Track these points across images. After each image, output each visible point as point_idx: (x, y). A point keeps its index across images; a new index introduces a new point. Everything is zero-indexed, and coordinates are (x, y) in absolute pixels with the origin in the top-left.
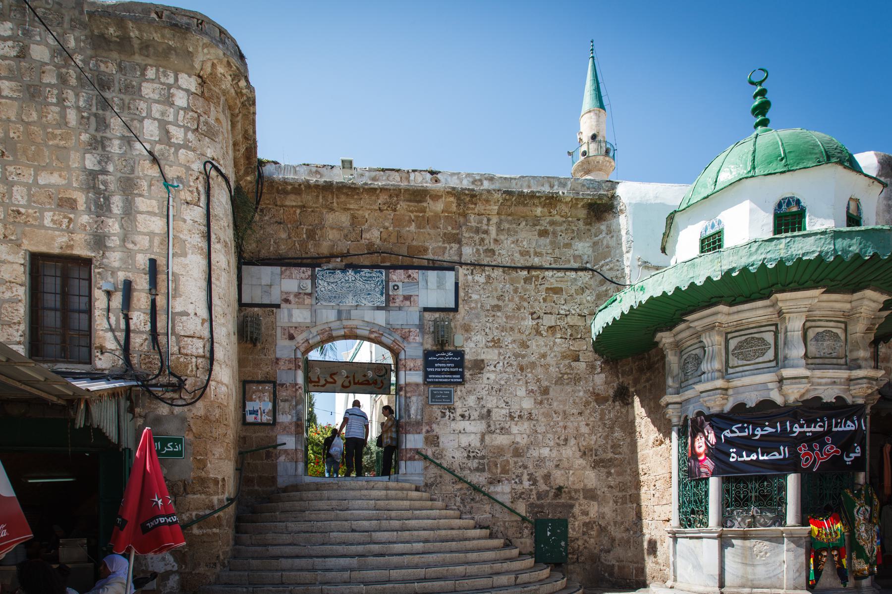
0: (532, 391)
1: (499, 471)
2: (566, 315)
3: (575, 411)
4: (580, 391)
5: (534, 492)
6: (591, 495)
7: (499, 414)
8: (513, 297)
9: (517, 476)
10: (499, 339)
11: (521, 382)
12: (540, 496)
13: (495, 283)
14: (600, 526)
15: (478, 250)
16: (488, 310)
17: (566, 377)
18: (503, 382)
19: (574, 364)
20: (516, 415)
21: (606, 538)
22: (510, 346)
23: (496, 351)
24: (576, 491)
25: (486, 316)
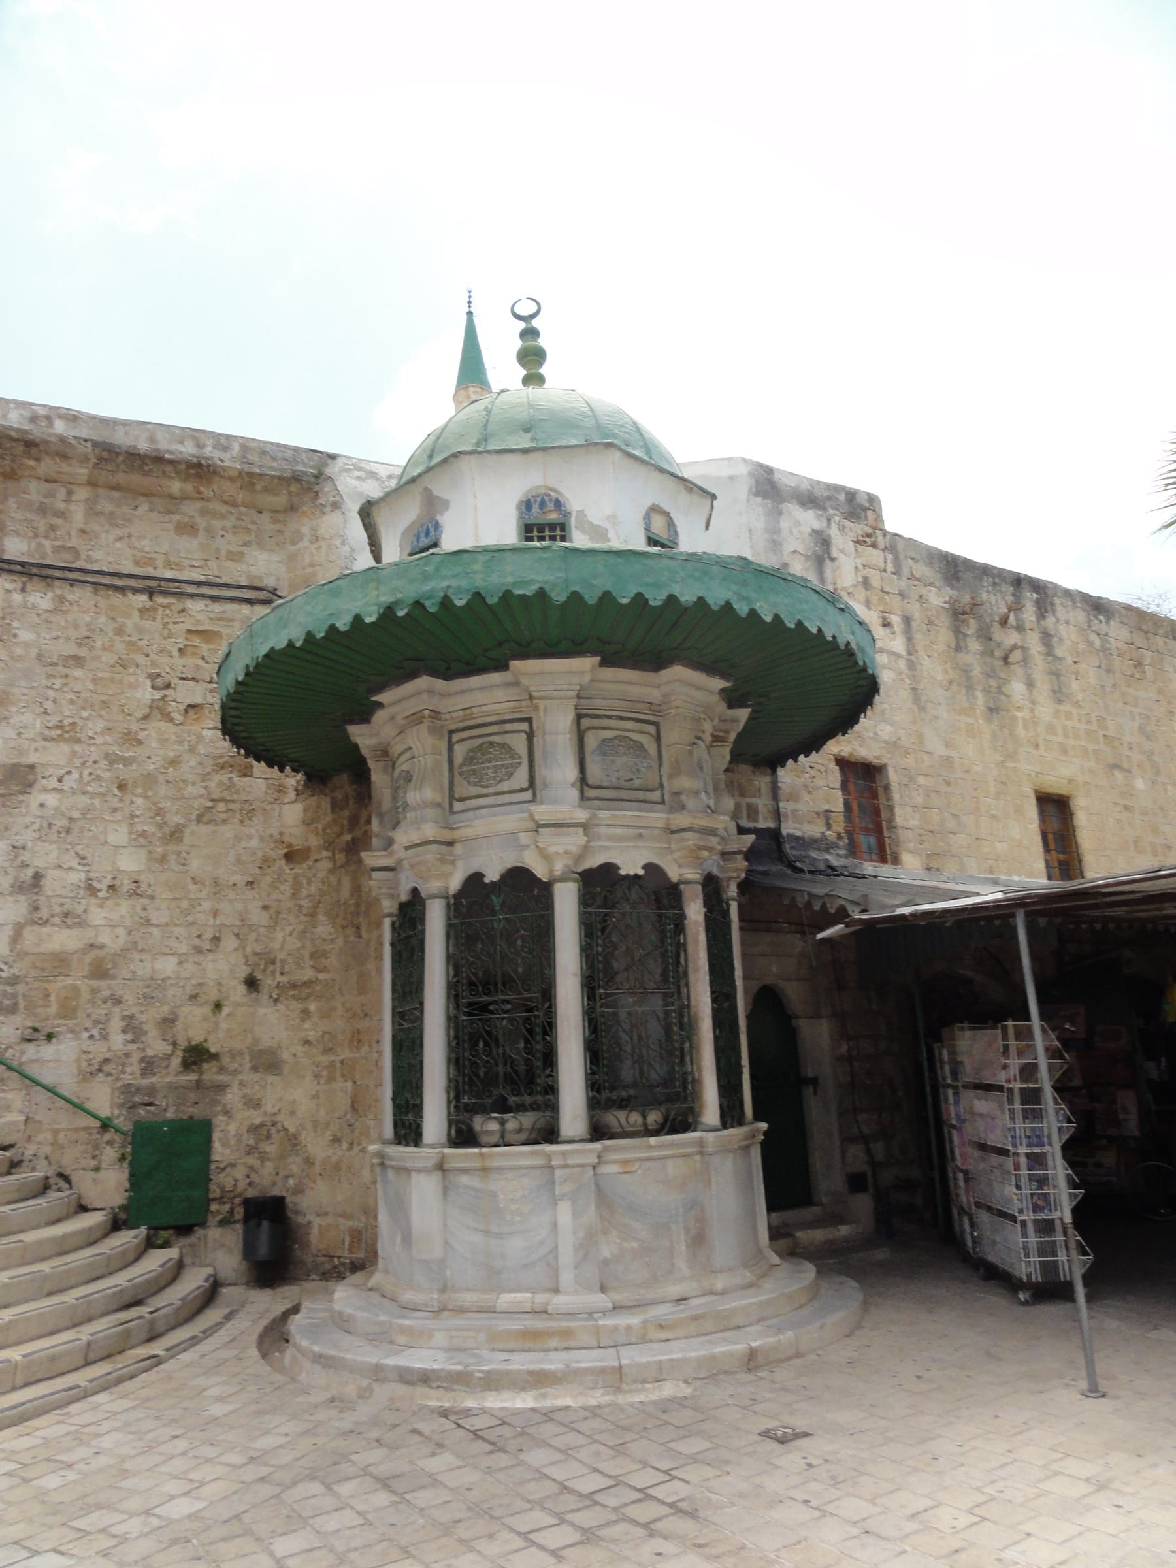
0: (143, 834)
1: (53, 1009)
3: (239, 879)
4: (250, 837)
5: (136, 1057)
6: (267, 1062)
7: (62, 882)
8: (112, 641)
9: (97, 1022)
10: (74, 724)
11: (118, 816)
12: (149, 1066)
14: (286, 1130)
15: (40, 545)
16: (54, 664)
17: (221, 806)
18: (76, 814)
20: (103, 886)
21: (299, 1160)
22: (99, 740)
23: (65, 748)
24: (233, 1055)
25: (50, 676)
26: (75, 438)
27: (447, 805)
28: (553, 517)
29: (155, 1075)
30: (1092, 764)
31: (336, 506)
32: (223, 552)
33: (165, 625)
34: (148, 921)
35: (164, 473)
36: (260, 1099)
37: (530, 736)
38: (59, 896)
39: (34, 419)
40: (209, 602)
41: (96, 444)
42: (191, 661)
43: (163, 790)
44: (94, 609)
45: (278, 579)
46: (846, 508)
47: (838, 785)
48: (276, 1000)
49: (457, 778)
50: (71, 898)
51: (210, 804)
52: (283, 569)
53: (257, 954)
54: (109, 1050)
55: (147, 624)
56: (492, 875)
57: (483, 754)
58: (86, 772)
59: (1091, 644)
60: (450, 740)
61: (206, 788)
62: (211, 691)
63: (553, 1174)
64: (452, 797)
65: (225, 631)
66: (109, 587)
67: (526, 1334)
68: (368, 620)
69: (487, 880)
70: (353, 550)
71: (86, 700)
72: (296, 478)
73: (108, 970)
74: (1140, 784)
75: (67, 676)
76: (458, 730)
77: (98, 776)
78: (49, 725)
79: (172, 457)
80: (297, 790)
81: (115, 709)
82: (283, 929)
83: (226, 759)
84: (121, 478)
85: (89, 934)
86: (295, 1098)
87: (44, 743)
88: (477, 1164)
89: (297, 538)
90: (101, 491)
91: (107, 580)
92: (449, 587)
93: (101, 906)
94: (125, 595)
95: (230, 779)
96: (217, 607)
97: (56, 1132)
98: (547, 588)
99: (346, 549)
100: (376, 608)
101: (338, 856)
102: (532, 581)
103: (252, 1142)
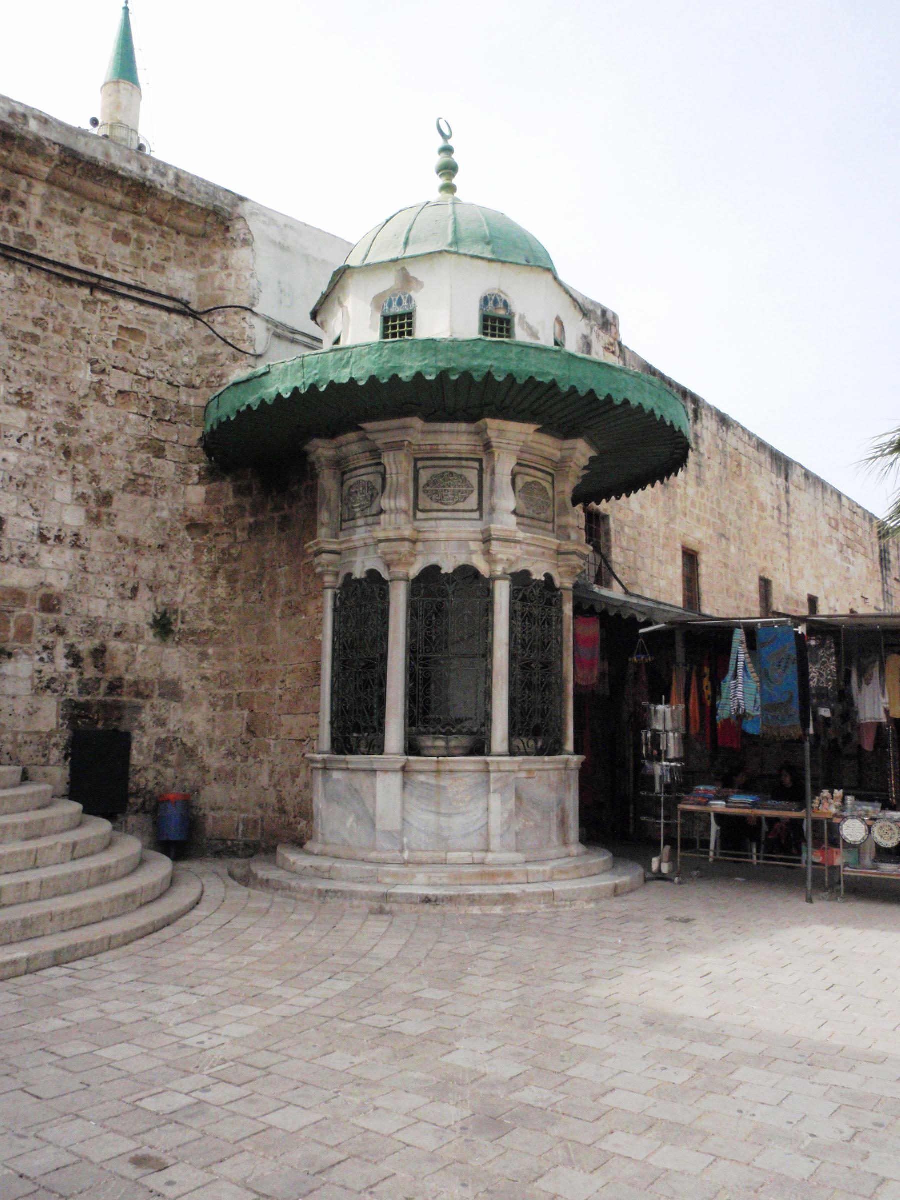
0: (83, 496)
2: (149, 379)
3: (154, 542)
4: (163, 509)
5: (75, 679)
6: (172, 691)
8: (62, 326)
10: (30, 393)
11: (64, 477)
13: (32, 296)
14: (185, 745)
16: (15, 338)
17: (141, 481)
18: (31, 472)
19: (157, 462)
20: (52, 535)
22: (50, 411)
23: (23, 414)
26: (48, 140)
27: (411, 514)
28: (502, 313)
29: (89, 694)
30: (711, 532)
31: (246, 243)
32: (150, 263)
33: (103, 318)
34: (85, 569)
35: (111, 185)
36: (165, 720)
37: (481, 472)
38: (18, 540)
39: (12, 114)
40: (137, 305)
41: (64, 149)
42: (120, 353)
43: (97, 459)
44: (46, 294)
45: (190, 295)
46: (601, 321)
47: (583, 527)
48: (178, 643)
49: (421, 494)
50: (28, 543)
51: (133, 477)
52: (194, 287)
53: (163, 604)
54: (55, 671)
55: (88, 316)
56: (448, 568)
57: (445, 480)
58: (39, 438)
59: (718, 446)
60: (415, 466)
61: (130, 463)
62: (137, 382)
63: (489, 777)
64: (416, 507)
65: (147, 331)
66: (59, 276)
67: (482, 875)
68: (428, 378)
69: (443, 572)
70: (260, 284)
71: (40, 374)
72: (216, 212)
73: (54, 606)
74: (733, 550)
75: (25, 350)
76: (423, 459)
77: (48, 441)
78: (12, 391)
79: (124, 174)
80: (199, 474)
81: (63, 385)
82: (185, 586)
83: (146, 441)
84: (75, 181)
85: (41, 574)
86: (194, 719)
87: (7, 407)
88: (433, 767)
89: (207, 260)
90: (55, 190)
91: (58, 270)
92: (492, 366)
93: (50, 552)
94: (72, 286)
95: (148, 458)
96: (144, 310)
97: (16, 734)
98: (557, 379)
99: (254, 282)
100: (434, 370)
101: (239, 534)
102: (548, 374)
103: (159, 752)
